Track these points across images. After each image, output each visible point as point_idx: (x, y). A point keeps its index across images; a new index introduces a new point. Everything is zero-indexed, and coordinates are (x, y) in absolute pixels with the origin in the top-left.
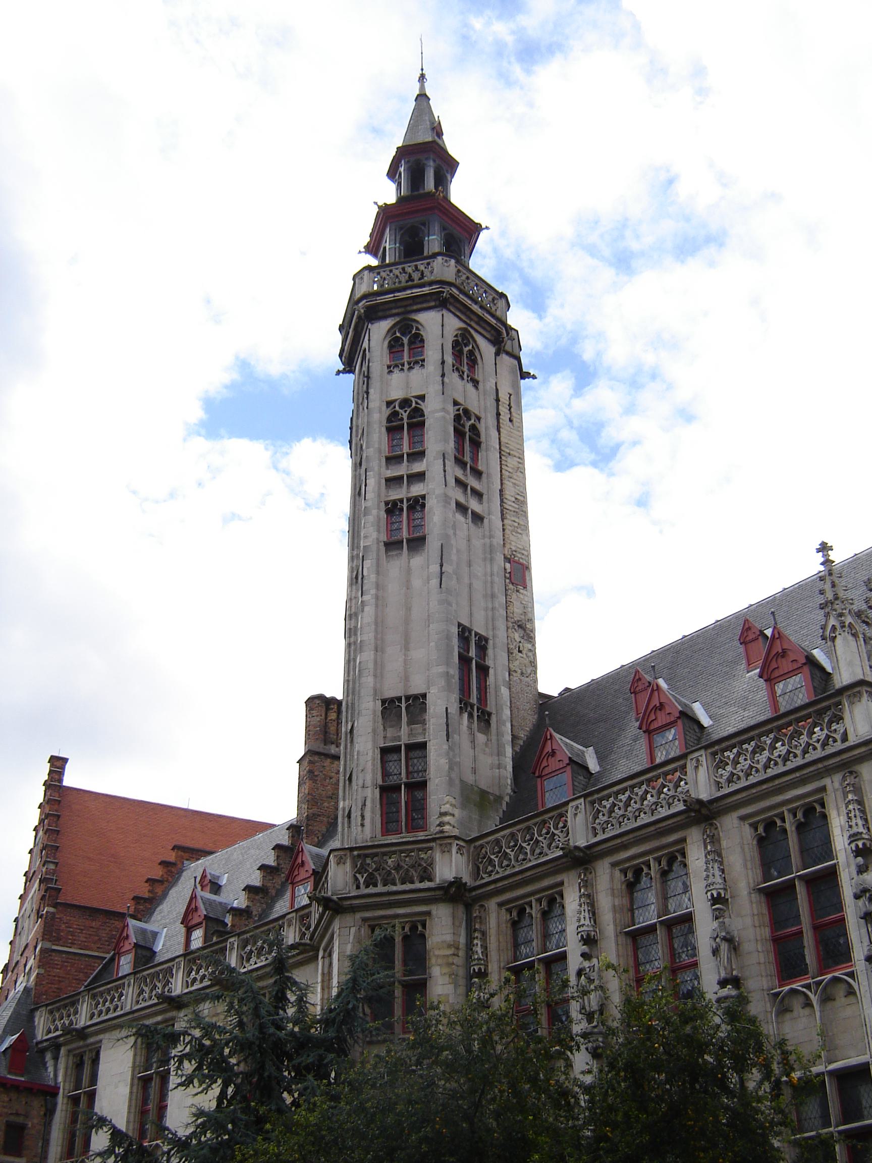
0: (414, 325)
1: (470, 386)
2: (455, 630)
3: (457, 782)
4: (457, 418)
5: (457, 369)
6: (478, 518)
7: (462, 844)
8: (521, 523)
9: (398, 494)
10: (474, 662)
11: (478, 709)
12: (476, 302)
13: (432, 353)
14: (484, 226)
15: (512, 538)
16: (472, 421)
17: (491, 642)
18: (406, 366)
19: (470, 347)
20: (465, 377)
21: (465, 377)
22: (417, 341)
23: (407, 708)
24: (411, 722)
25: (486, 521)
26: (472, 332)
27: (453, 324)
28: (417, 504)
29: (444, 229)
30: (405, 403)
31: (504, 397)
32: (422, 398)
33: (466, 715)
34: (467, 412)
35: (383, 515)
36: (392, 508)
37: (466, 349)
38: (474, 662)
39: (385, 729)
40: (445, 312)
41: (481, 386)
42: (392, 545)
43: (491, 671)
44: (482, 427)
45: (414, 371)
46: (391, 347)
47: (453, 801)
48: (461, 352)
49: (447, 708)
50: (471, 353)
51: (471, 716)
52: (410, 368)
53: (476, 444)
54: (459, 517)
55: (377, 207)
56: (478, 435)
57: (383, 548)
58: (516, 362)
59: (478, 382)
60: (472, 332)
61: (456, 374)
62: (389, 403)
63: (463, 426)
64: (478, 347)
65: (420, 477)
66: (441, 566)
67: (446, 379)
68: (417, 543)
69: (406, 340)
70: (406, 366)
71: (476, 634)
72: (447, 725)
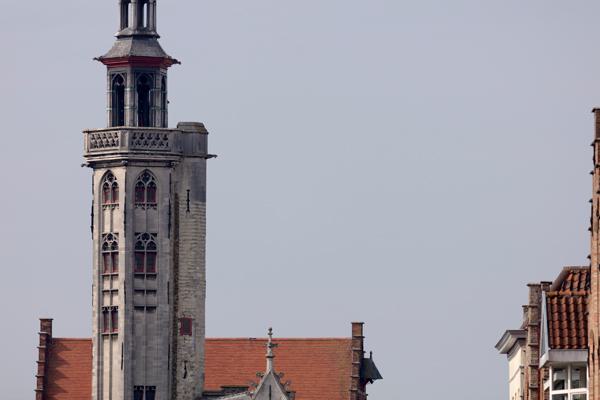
1: (151, 210)
2: (130, 393)
4: (138, 245)
6: (151, 309)
9: (107, 302)
13: (121, 201)
16: (150, 240)
21: (146, 207)
26: (150, 169)
27: (137, 171)
28: (115, 310)
29: (138, 74)
30: (110, 237)
31: (183, 196)
32: (117, 234)
34: (146, 236)
35: (102, 315)
36: (105, 311)
37: (147, 184)
46: (105, 189)
48: (143, 188)
50: (152, 183)
53: (153, 256)
54: (139, 314)
56: (155, 248)
61: (140, 208)
62: (104, 235)
63: (143, 248)
65: (114, 292)
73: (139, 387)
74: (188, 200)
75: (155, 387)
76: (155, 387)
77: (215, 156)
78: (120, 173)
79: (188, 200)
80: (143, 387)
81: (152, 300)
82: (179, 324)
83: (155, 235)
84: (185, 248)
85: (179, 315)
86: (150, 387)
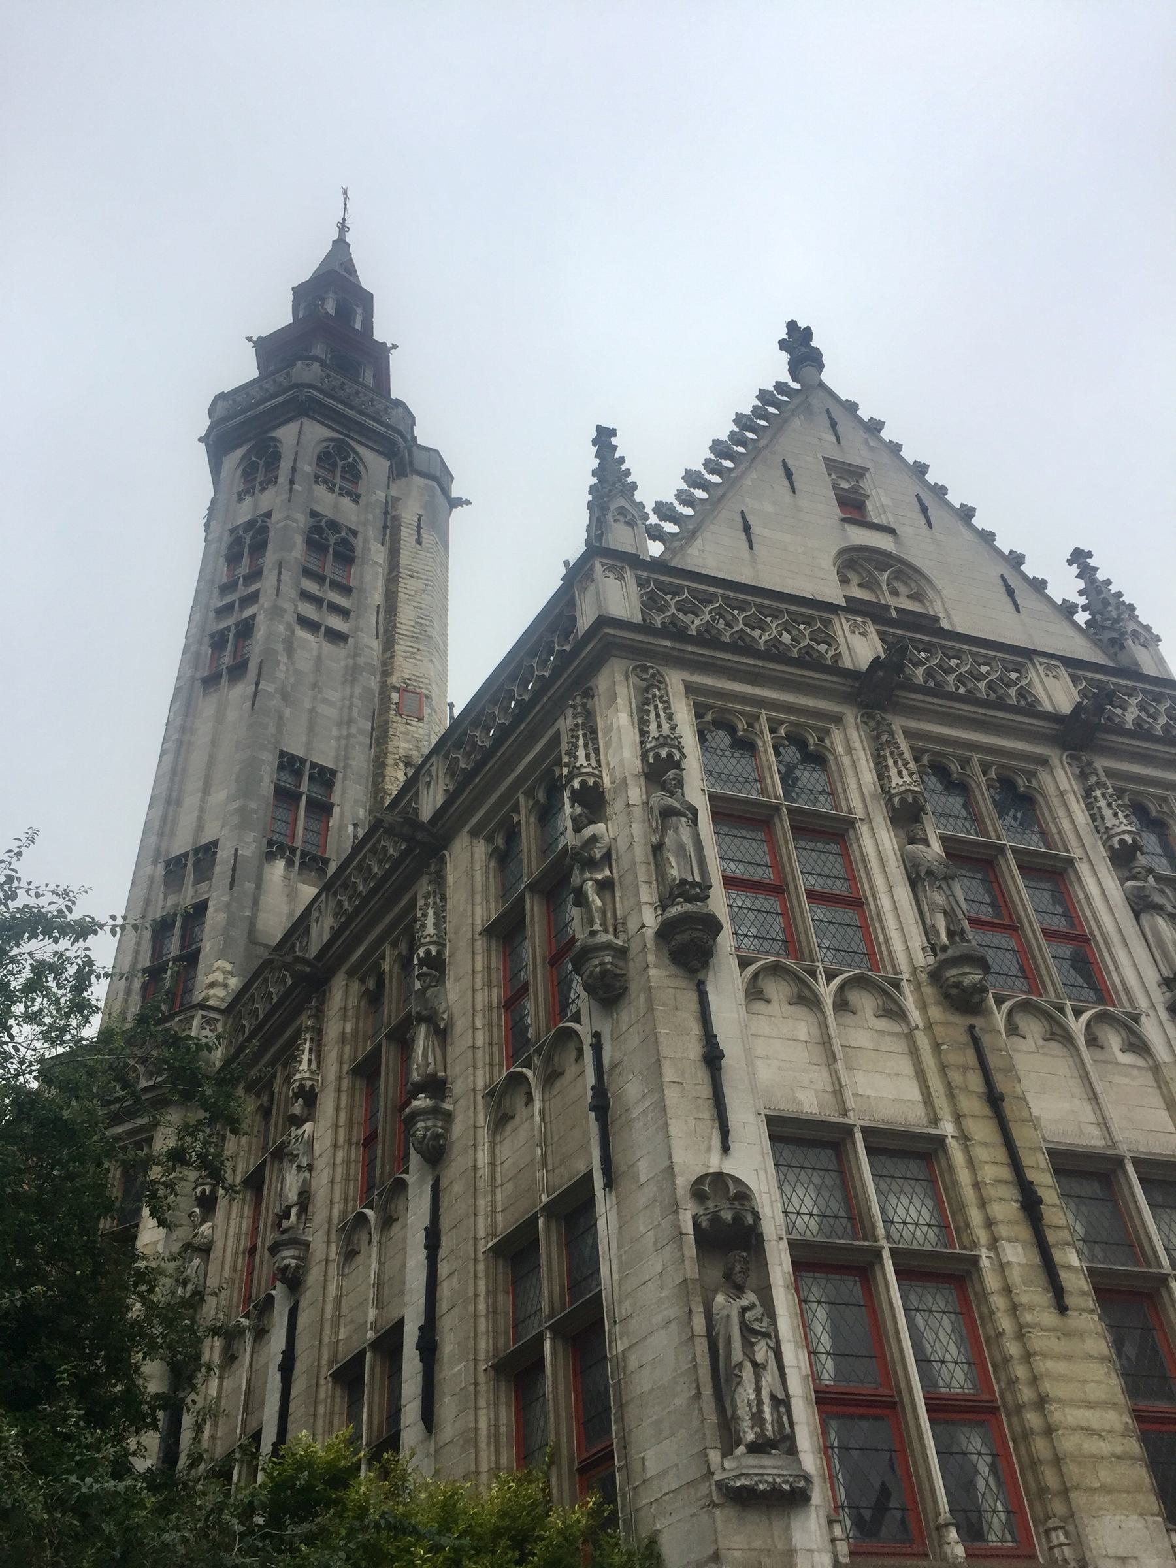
0: (272, 444)
2: (269, 759)
3: (242, 942)
5: (325, 482)
6: (336, 637)
7: (216, 1016)
8: (422, 648)
10: (304, 797)
11: (304, 854)
12: (352, 408)
14: (389, 345)
15: (406, 665)
17: (340, 775)
18: (258, 487)
19: (350, 460)
20: (337, 489)
22: (274, 459)
23: (195, 864)
24: (198, 881)
25: (351, 640)
26: (353, 443)
33: (280, 865)
34: (334, 526)
38: (304, 797)
39: (165, 899)
40: (305, 420)
41: (363, 500)
42: (211, 681)
43: (336, 810)
44: (358, 543)
45: (266, 492)
47: (228, 967)
49: (236, 850)
51: (290, 863)
52: (263, 489)
53: (346, 555)
55: (252, 344)
57: (198, 684)
58: (435, 484)
59: (358, 496)
60: (353, 443)
64: (361, 459)
66: (257, 684)
67: (297, 487)
68: (238, 670)
69: (261, 463)
70: (258, 487)
71: (313, 765)
72: (234, 870)
73: (293, 759)
74: (419, 527)
75: (333, 773)
76: (333, 773)
77: (468, 503)
78: (287, 434)
79: (419, 527)
80: (303, 761)
81: (336, 623)
82: (395, 696)
83: (355, 533)
84: (408, 587)
85: (394, 680)
86: (323, 770)
